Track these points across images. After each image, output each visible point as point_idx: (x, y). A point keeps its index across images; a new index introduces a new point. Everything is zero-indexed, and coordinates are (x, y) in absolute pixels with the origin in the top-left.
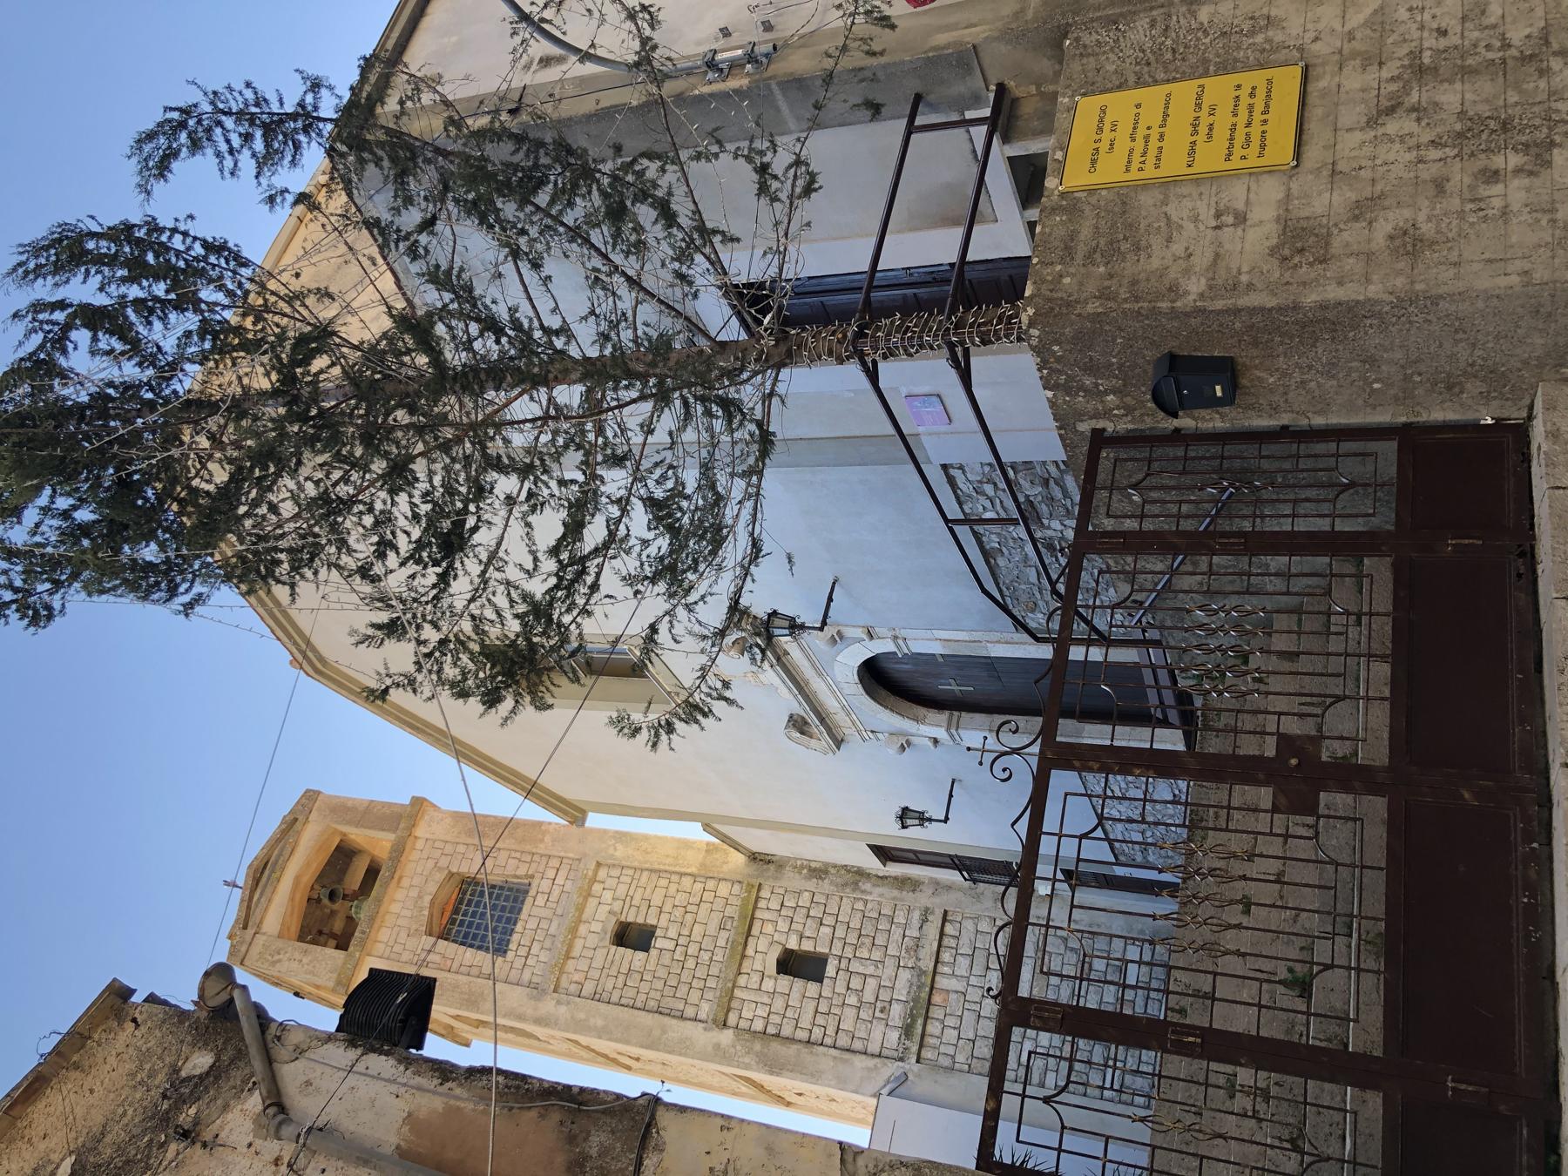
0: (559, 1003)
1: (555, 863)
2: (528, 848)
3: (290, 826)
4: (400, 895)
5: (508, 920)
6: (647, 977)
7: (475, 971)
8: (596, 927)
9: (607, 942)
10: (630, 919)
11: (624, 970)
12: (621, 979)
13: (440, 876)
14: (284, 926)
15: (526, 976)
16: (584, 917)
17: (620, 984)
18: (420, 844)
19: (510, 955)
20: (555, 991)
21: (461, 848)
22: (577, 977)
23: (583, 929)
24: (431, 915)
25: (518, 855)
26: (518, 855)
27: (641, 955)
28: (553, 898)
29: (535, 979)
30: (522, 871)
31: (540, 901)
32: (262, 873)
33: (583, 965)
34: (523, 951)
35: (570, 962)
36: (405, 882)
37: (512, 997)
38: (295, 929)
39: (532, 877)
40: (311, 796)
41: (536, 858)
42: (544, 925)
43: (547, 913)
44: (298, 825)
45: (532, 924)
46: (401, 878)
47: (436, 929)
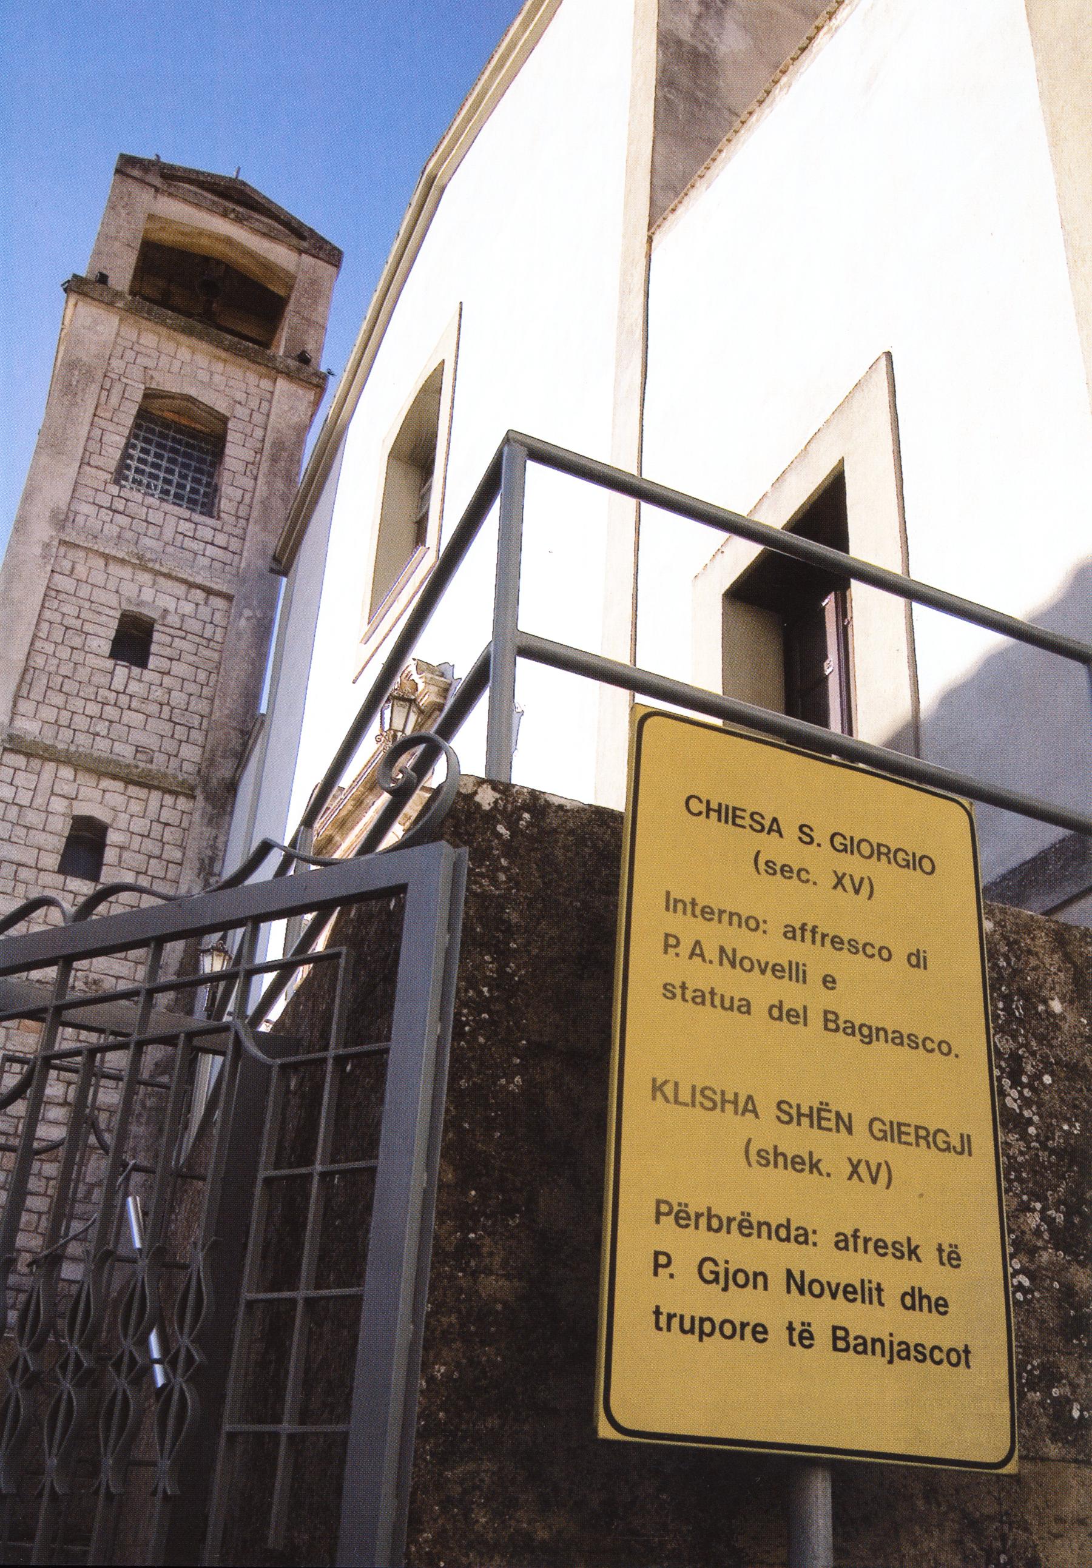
0: (47, 545)
1: (235, 544)
2: (255, 513)
3: (296, 233)
4: (201, 360)
5: (166, 492)
6: (78, 656)
7: (93, 446)
8: (147, 595)
9: (125, 606)
10: (156, 636)
11: (88, 628)
12: (77, 624)
13: (221, 406)
14: (167, 223)
15: (85, 508)
16: (161, 580)
17: (71, 622)
18: (266, 384)
19: (114, 490)
20: (63, 543)
21: (259, 433)
22: (81, 571)
23: (145, 578)
24: (171, 396)
25: (247, 501)
26: (247, 501)
27: (106, 648)
28: (188, 543)
29: (80, 519)
30: (225, 505)
31: (185, 527)
32: (234, 197)
33: (99, 578)
34: (119, 505)
35: (101, 562)
36: (219, 367)
37: (57, 493)
38: (167, 237)
39: (219, 518)
40: (333, 256)
41: (243, 522)
42: (152, 530)
43: (168, 533)
44: (295, 241)
45: (155, 517)
46: (225, 361)
47: (155, 405)
